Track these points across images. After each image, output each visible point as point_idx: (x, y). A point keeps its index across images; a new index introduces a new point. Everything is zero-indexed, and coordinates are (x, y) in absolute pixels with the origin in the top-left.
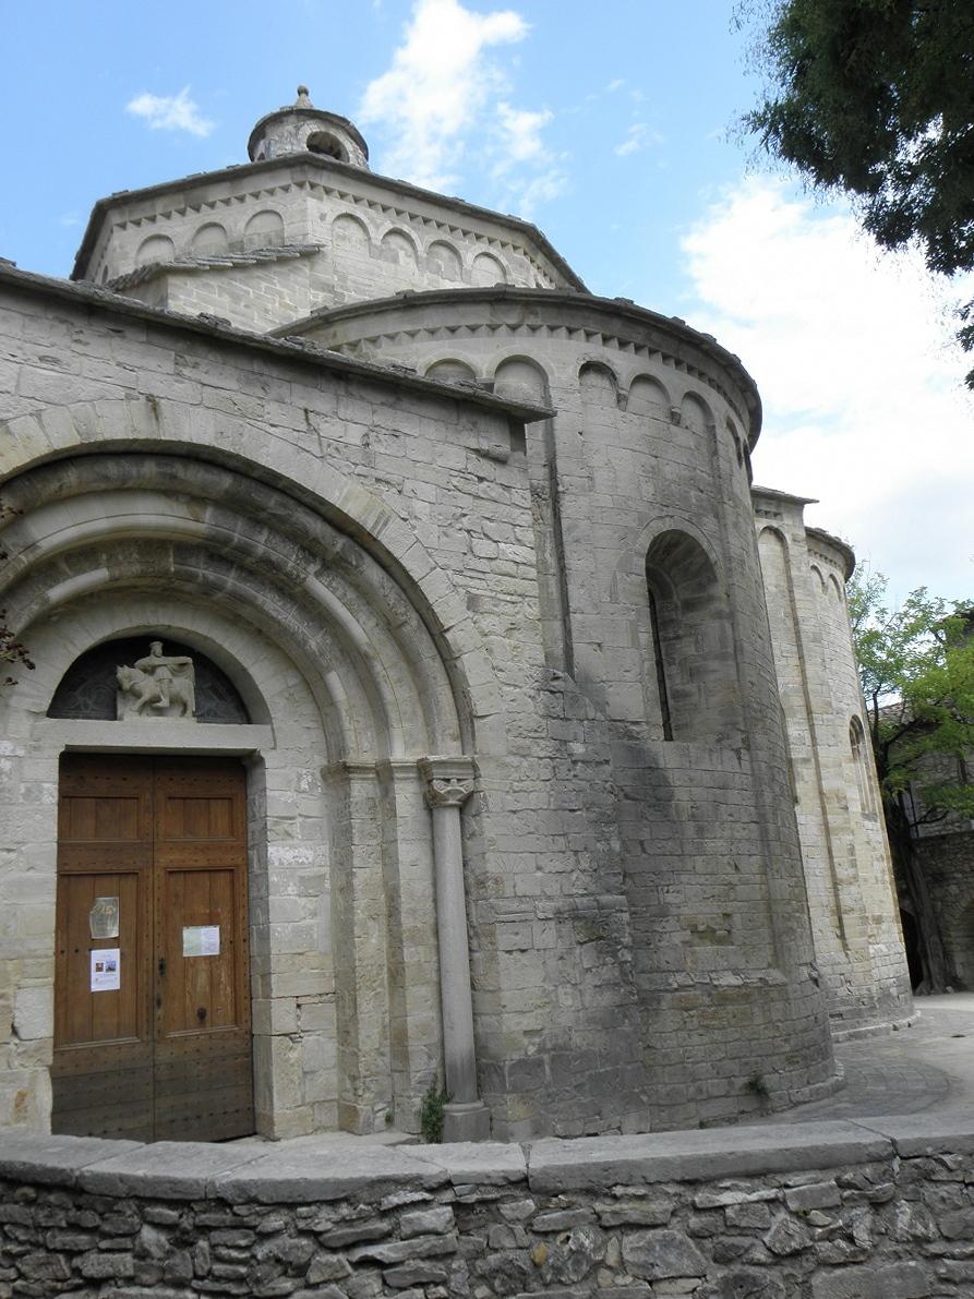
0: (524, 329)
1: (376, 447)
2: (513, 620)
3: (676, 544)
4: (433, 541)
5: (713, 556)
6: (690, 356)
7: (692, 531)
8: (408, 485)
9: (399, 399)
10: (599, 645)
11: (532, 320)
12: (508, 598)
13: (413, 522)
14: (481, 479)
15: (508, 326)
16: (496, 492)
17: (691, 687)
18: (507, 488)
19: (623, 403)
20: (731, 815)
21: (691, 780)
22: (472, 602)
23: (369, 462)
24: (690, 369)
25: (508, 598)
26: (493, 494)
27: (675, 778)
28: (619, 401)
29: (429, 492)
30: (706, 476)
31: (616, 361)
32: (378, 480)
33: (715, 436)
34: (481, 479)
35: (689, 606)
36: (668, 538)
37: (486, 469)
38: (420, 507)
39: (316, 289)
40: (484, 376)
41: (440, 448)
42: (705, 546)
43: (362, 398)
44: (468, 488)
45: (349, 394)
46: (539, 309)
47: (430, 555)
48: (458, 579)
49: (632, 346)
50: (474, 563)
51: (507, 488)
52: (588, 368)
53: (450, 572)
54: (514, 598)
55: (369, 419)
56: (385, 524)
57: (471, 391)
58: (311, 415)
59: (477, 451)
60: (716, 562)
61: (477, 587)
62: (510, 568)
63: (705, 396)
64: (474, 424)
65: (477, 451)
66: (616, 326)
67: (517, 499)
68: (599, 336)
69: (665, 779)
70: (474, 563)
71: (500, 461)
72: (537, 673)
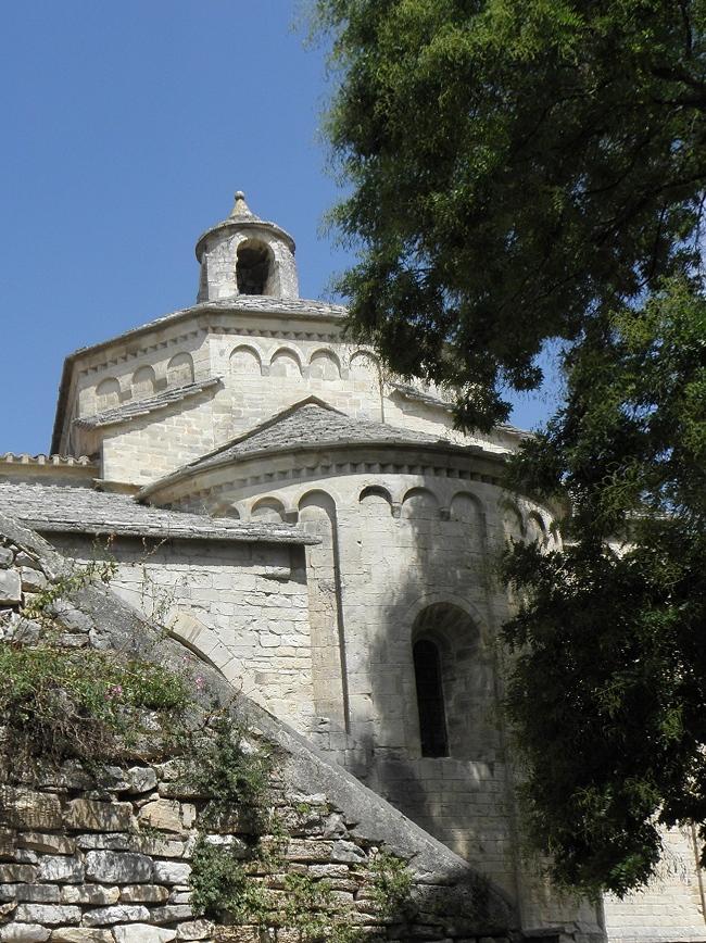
0: (319, 470)
1: (193, 585)
2: (291, 686)
3: (446, 612)
4: (232, 641)
5: (477, 618)
6: (460, 463)
7: (457, 601)
8: (213, 608)
9: (208, 550)
10: (369, 695)
11: (325, 462)
12: (287, 672)
13: (218, 630)
14: (268, 594)
15: (308, 468)
16: (280, 600)
17: (461, 717)
18: (288, 596)
19: (397, 513)
20: (479, 811)
21: (442, 787)
22: (259, 678)
23: (187, 596)
24: (462, 474)
25: (287, 672)
26: (277, 603)
27: (428, 786)
28: (392, 513)
29: (229, 609)
30: (475, 555)
31: (389, 482)
32: (193, 606)
33: (484, 520)
34: (268, 594)
35: (462, 655)
36: (437, 608)
37: (273, 585)
38: (221, 620)
39: (217, 412)
40: (291, 508)
41: (236, 578)
42: (469, 610)
43: (182, 554)
44: (257, 602)
45: (173, 553)
46: (329, 454)
47: (229, 650)
48: (249, 664)
49: (406, 468)
50: (260, 651)
51: (288, 596)
52: (368, 491)
53: (243, 660)
54: (291, 672)
55: (186, 567)
56: (198, 634)
57: (255, 538)
58: (147, 571)
59: (263, 576)
60: (479, 622)
61: (263, 667)
62: (291, 651)
63: (476, 492)
64: (262, 558)
65: (263, 576)
66: (391, 455)
67: (297, 602)
68: (378, 465)
69: (420, 787)
70: (260, 651)
71: (283, 579)
72: (308, 721)
